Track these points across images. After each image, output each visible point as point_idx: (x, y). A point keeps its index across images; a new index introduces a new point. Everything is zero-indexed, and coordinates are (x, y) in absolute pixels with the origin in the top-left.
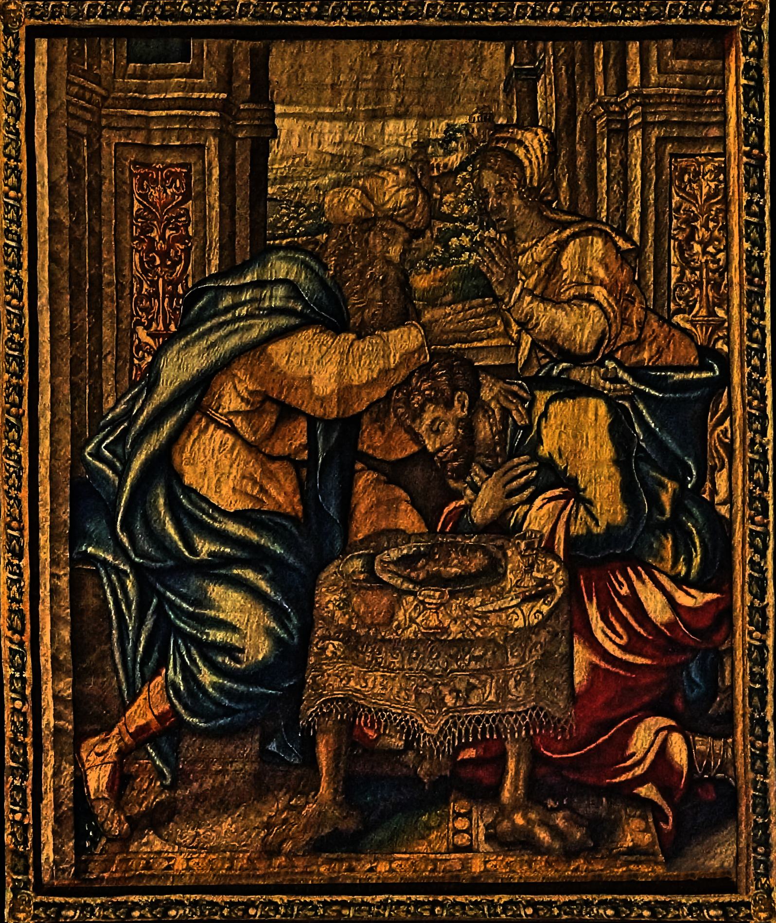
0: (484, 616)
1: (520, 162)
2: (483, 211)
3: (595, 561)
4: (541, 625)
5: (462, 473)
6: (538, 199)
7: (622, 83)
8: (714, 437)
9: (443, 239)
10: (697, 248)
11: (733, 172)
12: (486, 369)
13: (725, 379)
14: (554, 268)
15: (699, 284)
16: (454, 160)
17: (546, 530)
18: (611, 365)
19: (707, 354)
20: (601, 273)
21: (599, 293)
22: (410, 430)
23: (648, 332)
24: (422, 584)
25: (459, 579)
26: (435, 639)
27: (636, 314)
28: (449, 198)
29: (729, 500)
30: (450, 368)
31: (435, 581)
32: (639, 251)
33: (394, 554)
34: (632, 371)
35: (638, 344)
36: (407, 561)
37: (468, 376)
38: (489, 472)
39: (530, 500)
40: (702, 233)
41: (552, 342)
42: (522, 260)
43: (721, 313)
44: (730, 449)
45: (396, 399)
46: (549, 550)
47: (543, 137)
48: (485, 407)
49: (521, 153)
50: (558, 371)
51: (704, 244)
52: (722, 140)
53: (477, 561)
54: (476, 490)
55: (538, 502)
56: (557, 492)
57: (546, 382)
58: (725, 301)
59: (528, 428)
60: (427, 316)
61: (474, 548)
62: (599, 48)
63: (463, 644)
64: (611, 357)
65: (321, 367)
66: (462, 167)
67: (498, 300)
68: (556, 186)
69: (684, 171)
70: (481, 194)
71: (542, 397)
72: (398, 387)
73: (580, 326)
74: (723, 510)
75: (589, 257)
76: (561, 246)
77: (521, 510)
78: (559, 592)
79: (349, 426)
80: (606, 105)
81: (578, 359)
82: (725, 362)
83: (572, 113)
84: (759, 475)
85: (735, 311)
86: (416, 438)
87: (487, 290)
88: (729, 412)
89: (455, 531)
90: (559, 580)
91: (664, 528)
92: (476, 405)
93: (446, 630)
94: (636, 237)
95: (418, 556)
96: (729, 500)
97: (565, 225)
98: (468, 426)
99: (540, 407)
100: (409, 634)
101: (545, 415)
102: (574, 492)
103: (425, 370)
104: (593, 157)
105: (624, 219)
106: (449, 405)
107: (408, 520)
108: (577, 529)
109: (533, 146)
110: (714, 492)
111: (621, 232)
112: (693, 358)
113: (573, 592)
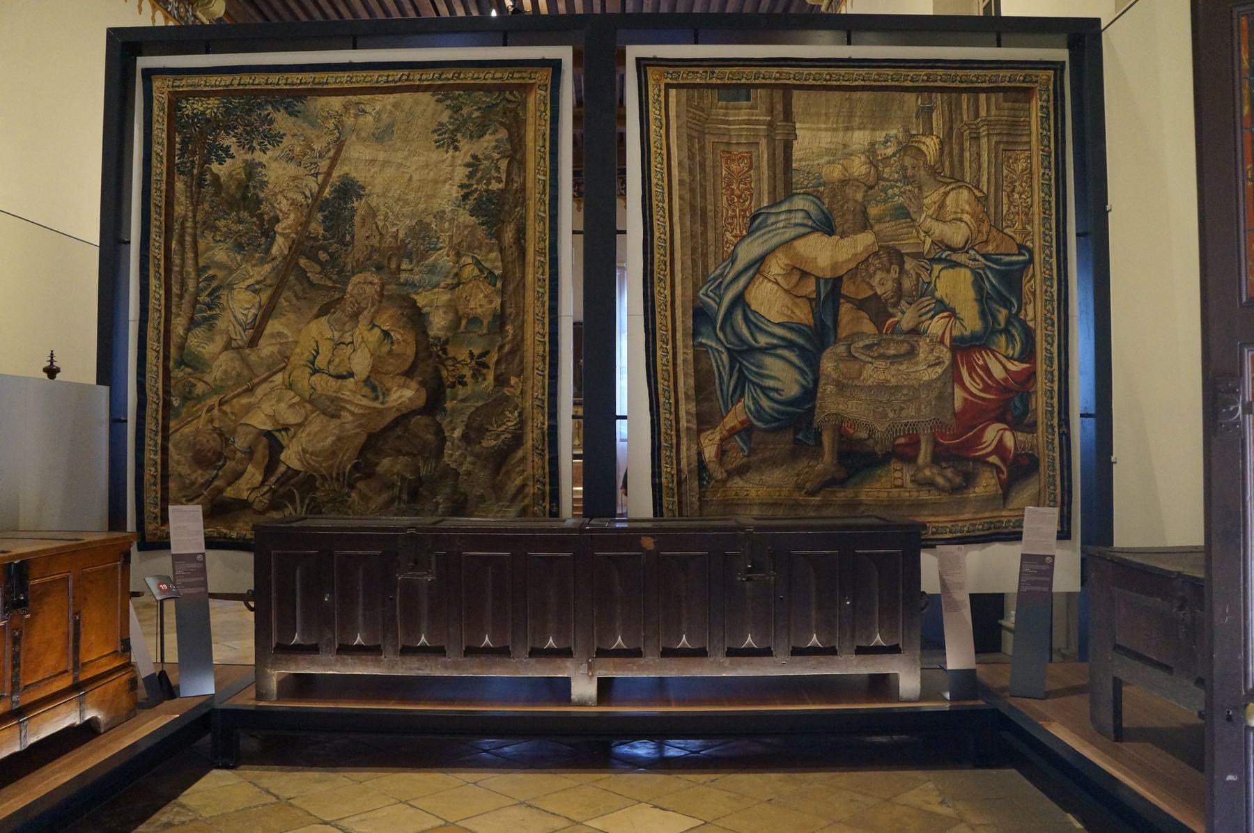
0: (908, 374)
1: (923, 152)
2: (905, 177)
3: (964, 347)
4: (938, 379)
5: (896, 305)
6: (934, 172)
7: (977, 115)
8: (1026, 288)
9: (885, 190)
10: (1016, 196)
11: (1035, 159)
12: (907, 254)
13: (1031, 261)
14: (942, 205)
15: (1018, 213)
16: (890, 151)
17: (940, 333)
18: (972, 252)
19: (1022, 248)
20: (967, 208)
21: (966, 217)
22: (868, 284)
23: (991, 237)
24: (876, 358)
25: (895, 356)
26: (882, 386)
27: (985, 228)
28: (887, 170)
29: (1035, 319)
30: (889, 253)
31: (882, 357)
32: (986, 197)
33: (861, 344)
34: (985, 256)
35: (986, 242)
36: (868, 347)
37: (897, 257)
38: (910, 304)
39: (932, 318)
40: (1018, 189)
41: (942, 242)
42: (926, 201)
43: (1029, 228)
44: (1034, 294)
45: (860, 268)
46: (942, 342)
47: (937, 141)
48: (907, 273)
49: (924, 148)
50: (945, 255)
51: (1020, 194)
52: (1029, 142)
53: (904, 348)
54: (903, 313)
55: (936, 319)
56: (945, 314)
57: (940, 260)
58: (1030, 222)
59: (929, 283)
60: (876, 228)
61: (902, 342)
62: (965, 96)
63: (897, 388)
64: (972, 248)
65: (823, 253)
66: (894, 155)
67: (913, 220)
68: (943, 165)
69: (1009, 158)
70: (904, 168)
71: (937, 267)
72: (862, 262)
73: (957, 234)
74: (1031, 324)
75: (960, 200)
76: (946, 194)
77: (927, 323)
78: (947, 363)
79: (837, 282)
80: (968, 125)
81: (954, 250)
82: (1031, 252)
83: (951, 128)
84: (1049, 307)
85: (1036, 227)
86: (872, 287)
87: (908, 215)
88: (1033, 276)
89: (892, 333)
90: (946, 356)
91: (1001, 332)
92: (902, 270)
93: (888, 381)
94: (985, 190)
95: (874, 345)
96: (1035, 319)
97: (948, 184)
98: (899, 283)
99: (935, 273)
100: (869, 383)
101: (938, 277)
102: (953, 314)
103: (876, 254)
104: (962, 150)
105: (978, 181)
106: (888, 271)
107: (868, 327)
108: (956, 333)
109: (930, 145)
110: (1026, 315)
111: (977, 188)
112: (1015, 250)
113: (954, 364)
